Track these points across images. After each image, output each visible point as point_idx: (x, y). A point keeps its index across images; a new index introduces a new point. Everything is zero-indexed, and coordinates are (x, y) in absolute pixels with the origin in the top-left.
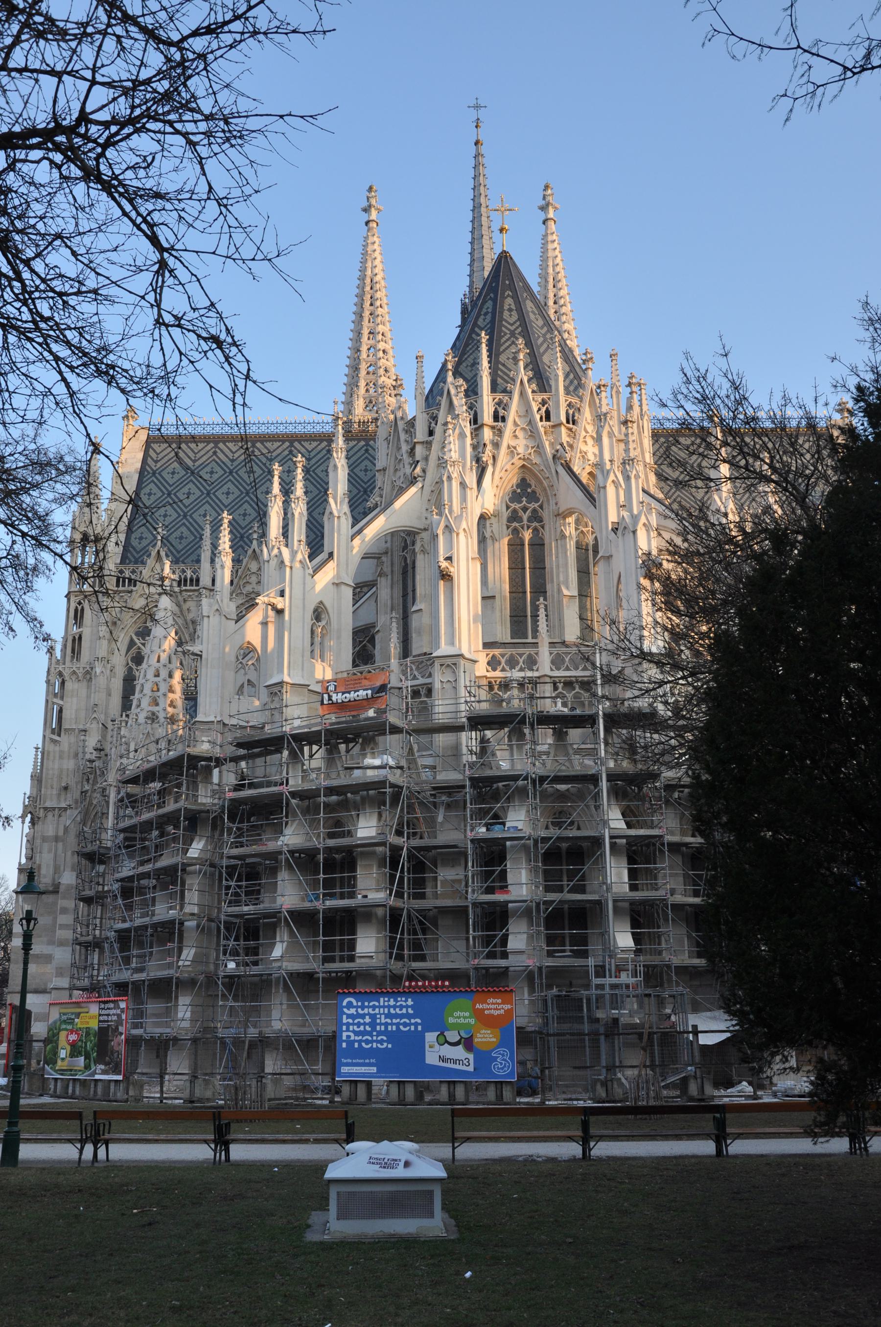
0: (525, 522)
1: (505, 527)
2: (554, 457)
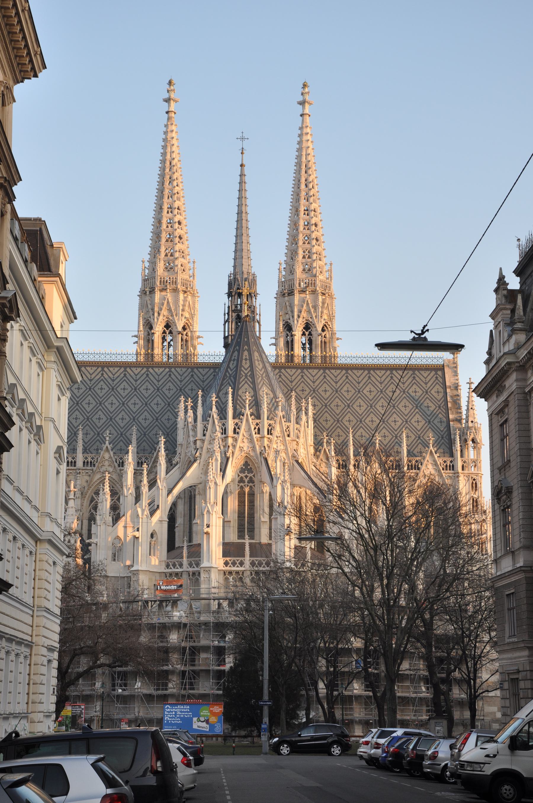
0: (246, 483)
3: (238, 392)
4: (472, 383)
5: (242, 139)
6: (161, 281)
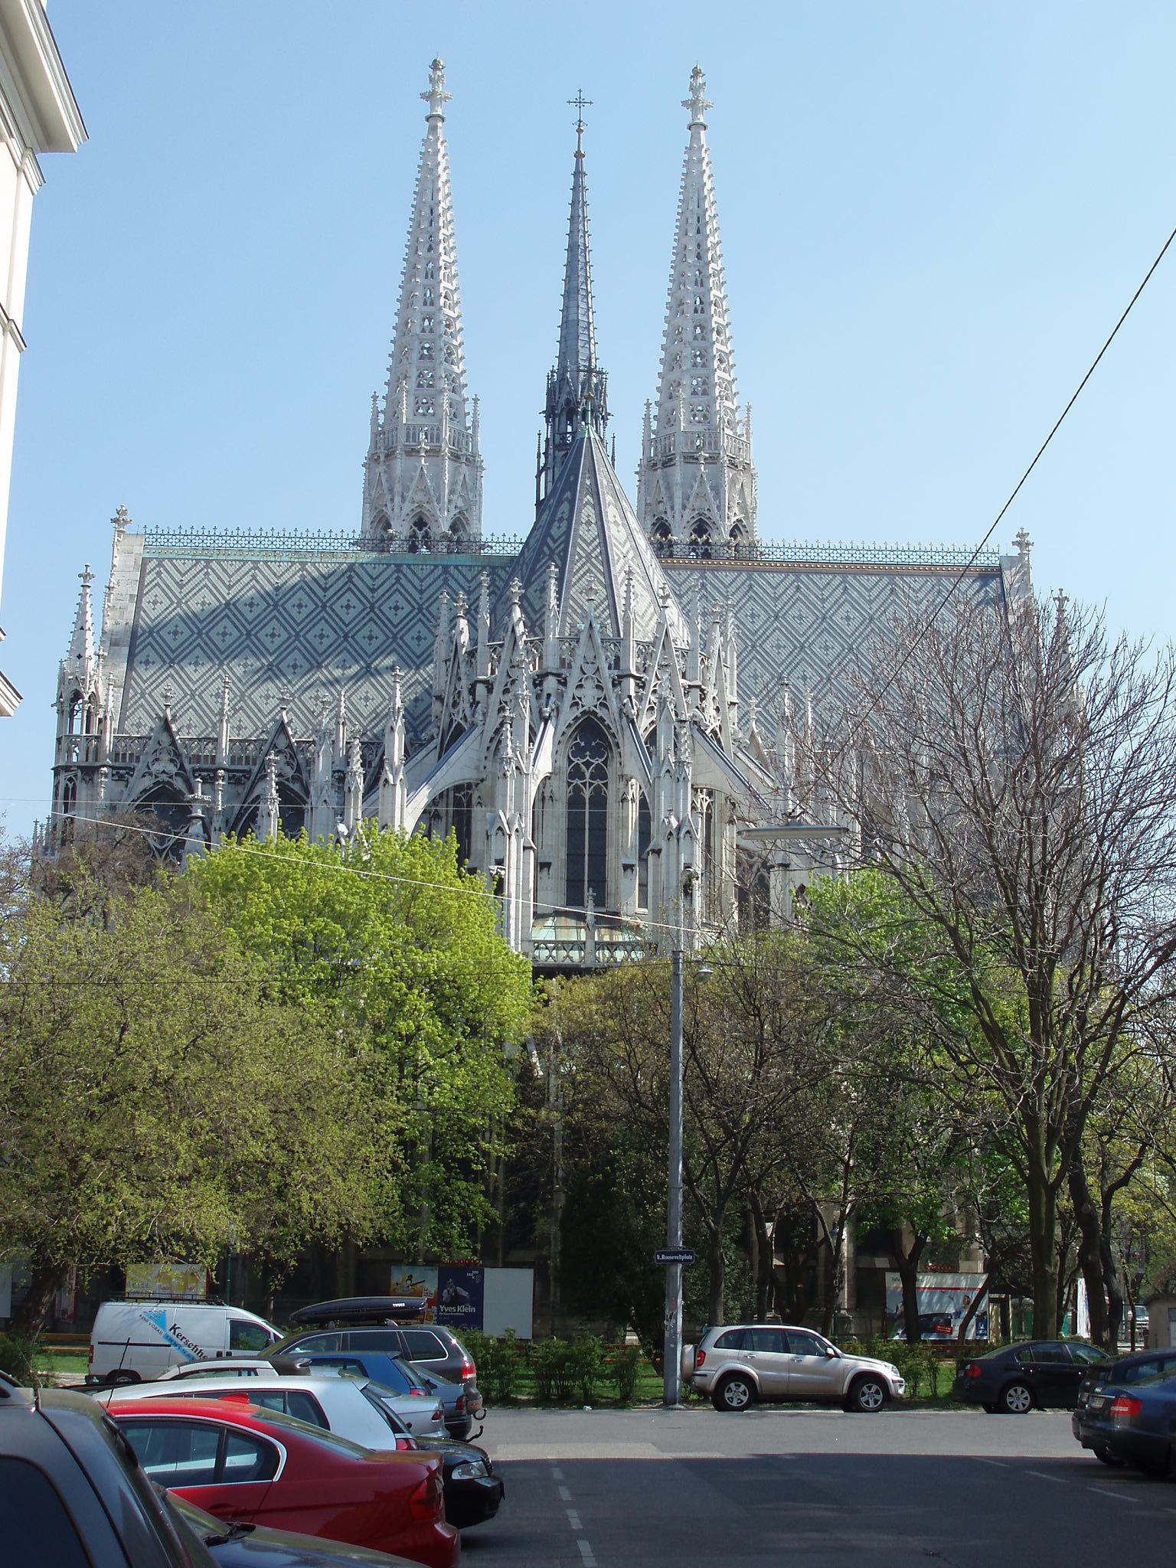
2: (621, 710)
3: (568, 592)
5: (580, 102)
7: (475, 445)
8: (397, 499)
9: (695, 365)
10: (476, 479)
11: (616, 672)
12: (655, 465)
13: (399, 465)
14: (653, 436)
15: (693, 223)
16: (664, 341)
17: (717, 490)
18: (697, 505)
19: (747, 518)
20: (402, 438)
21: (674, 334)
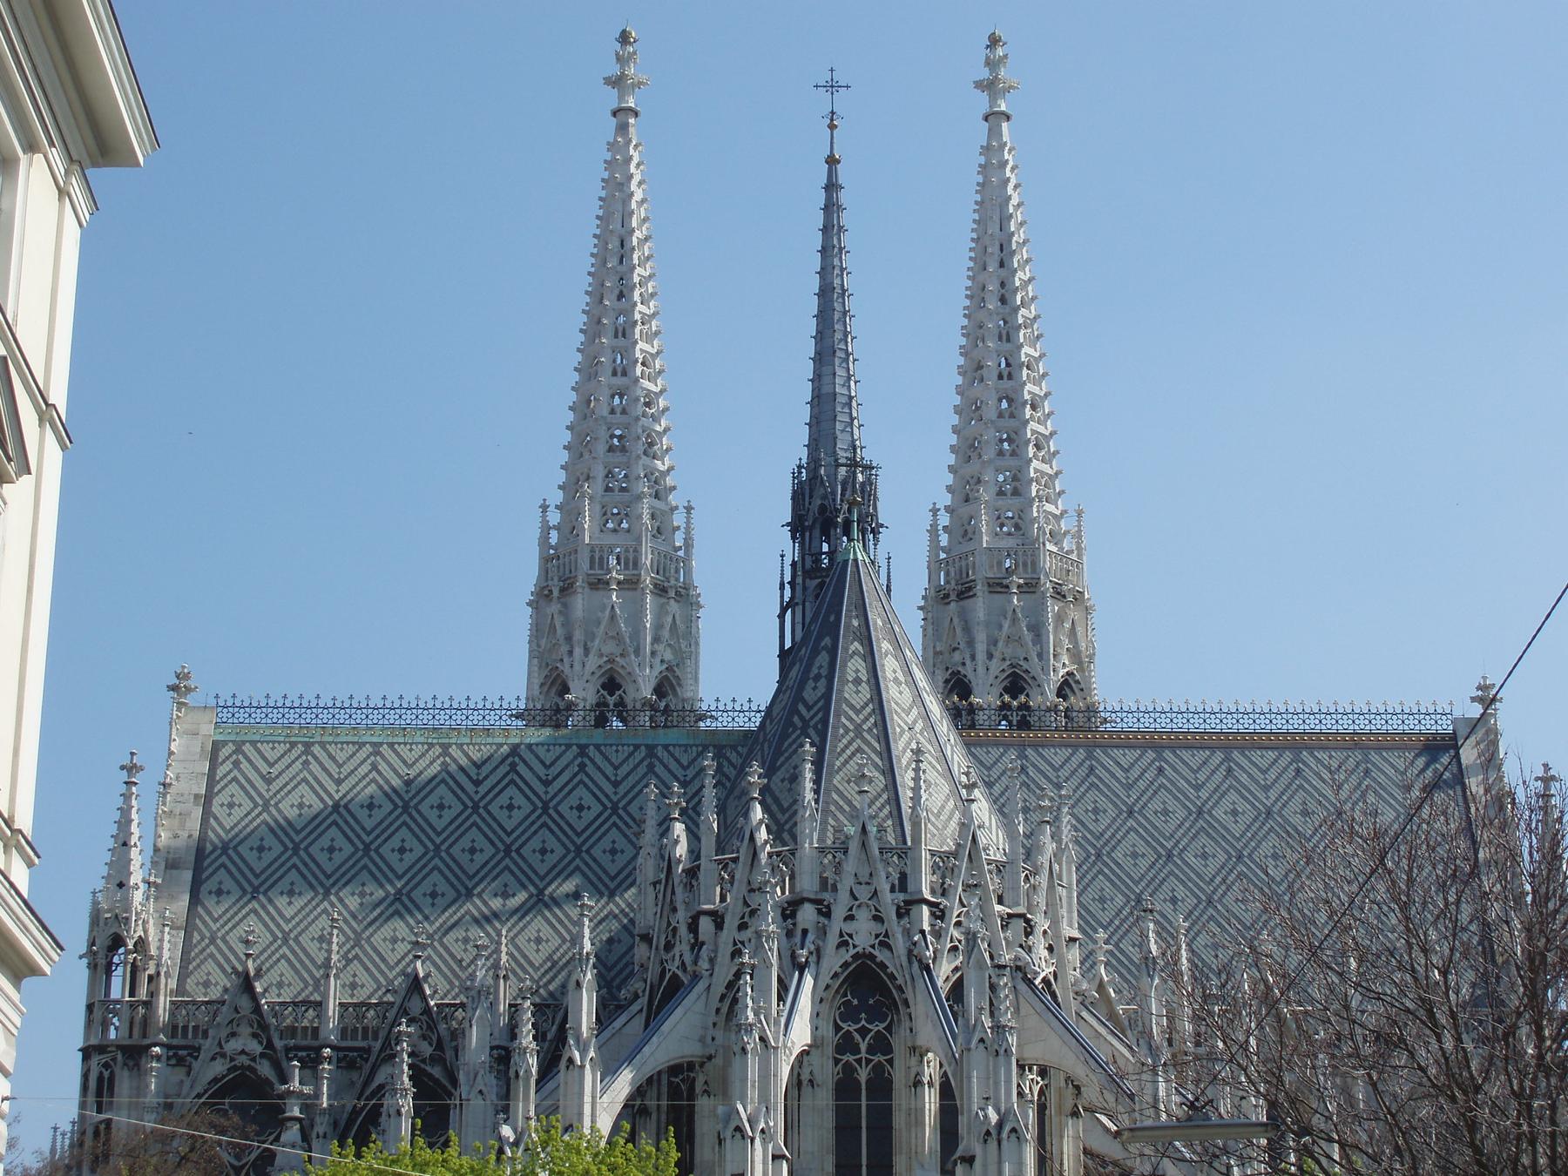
0: (863, 1054)
1: (831, 1062)
2: (910, 952)
3: (829, 781)
4: (1553, 778)
5: (832, 87)
6: (592, 559)
7: (688, 572)
8: (578, 651)
9: (1001, 453)
10: (691, 621)
11: (902, 897)
12: (947, 596)
13: (580, 603)
14: (943, 556)
15: (994, 253)
16: (955, 420)
17: (1037, 630)
18: (1008, 652)
19: (1081, 669)
20: (584, 565)
21: (970, 409)
